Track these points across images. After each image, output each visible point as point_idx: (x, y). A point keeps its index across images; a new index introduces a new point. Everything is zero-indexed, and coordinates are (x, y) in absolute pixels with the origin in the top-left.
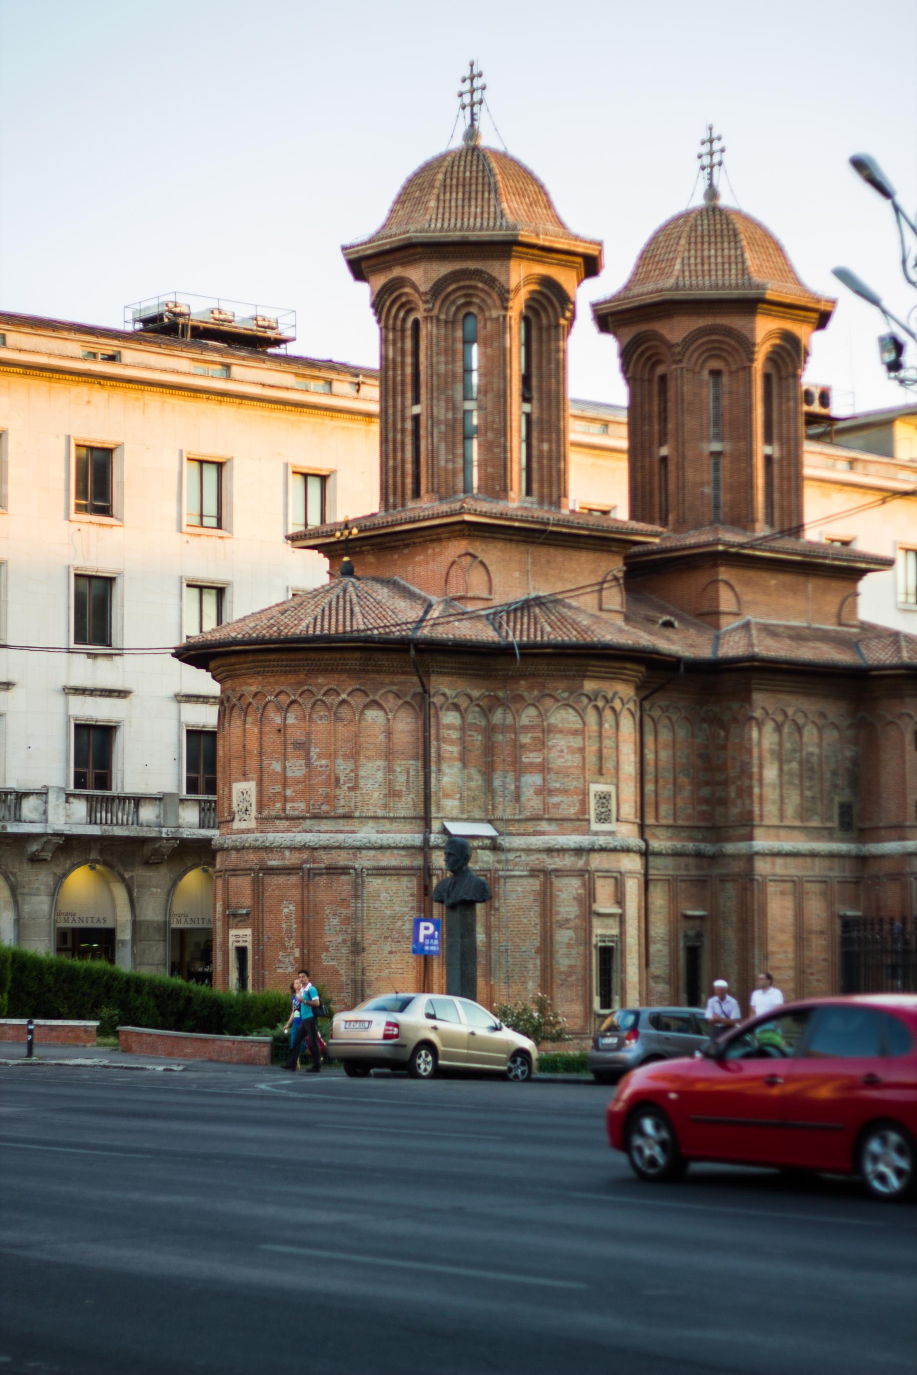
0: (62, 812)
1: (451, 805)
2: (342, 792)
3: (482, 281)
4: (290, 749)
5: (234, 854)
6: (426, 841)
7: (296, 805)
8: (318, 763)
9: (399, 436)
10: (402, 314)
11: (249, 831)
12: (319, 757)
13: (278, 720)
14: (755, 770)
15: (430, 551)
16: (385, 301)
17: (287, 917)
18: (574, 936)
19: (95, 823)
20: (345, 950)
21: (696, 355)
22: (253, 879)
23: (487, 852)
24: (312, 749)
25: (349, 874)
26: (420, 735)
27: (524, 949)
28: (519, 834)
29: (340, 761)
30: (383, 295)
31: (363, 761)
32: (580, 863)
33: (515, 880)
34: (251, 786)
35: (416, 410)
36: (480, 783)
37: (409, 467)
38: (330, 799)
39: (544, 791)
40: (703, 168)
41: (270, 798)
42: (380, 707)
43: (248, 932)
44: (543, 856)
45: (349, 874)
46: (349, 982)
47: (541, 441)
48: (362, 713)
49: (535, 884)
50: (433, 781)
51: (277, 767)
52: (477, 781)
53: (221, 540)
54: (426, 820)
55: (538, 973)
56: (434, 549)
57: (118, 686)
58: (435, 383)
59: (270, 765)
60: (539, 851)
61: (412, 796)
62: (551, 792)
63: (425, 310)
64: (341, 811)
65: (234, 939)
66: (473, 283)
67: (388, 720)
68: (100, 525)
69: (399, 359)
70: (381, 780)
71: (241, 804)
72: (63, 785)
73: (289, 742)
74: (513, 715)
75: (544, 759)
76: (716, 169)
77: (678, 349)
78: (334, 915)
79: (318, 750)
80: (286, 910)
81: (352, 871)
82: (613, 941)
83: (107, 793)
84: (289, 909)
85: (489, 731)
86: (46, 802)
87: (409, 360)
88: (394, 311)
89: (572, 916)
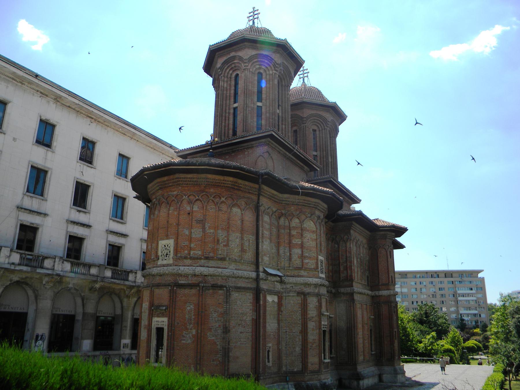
0: (60, 266)
1: (266, 259)
3: (267, 60)
5: (158, 278)
8: (209, 231)
9: (227, 115)
10: (231, 72)
11: (168, 265)
12: (210, 228)
13: (188, 209)
14: (352, 260)
15: (246, 153)
16: (225, 66)
17: (189, 312)
18: (314, 325)
19: (73, 273)
20: (220, 331)
21: (310, 123)
22: (170, 290)
23: (278, 284)
24: (206, 224)
25: (224, 290)
26: (255, 223)
27: (294, 332)
28: (291, 276)
29: (220, 231)
31: (231, 232)
32: (317, 291)
33: (290, 298)
34: (171, 242)
35: (235, 105)
36: (275, 251)
37: (231, 126)
39: (302, 257)
40: (300, 78)
41: (181, 248)
42: (239, 207)
43: (165, 319)
44: (302, 287)
45: (224, 290)
46: (221, 349)
47: (282, 124)
48: (231, 209)
49: (299, 300)
50: (260, 246)
52: (274, 251)
53: (126, 182)
54: (257, 264)
55: (301, 343)
56: (248, 152)
57: (87, 223)
58: (248, 92)
59: (183, 231)
60: (301, 284)
61: (251, 253)
62: (305, 257)
63: (245, 66)
64: (219, 256)
65: (156, 323)
66: (263, 60)
67: (242, 214)
68: (88, 166)
69: (228, 88)
70: (238, 243)
71: (163, 253)
72: (62, 256)
73: (194, 219)
74: (289, 221)
75: (302, 242)
76: (306, 79)
77: (305, 119)
78: (215, 311)
79: (209, 225)
80: (189, 308)
81: (225, 289)
82: (325, 328)
83: (79, 261)
84: (190, 307)
85: (279, 228)
86: (55, 262)
87: (233, 88)
88: (228, 70)
89: (314, 316)
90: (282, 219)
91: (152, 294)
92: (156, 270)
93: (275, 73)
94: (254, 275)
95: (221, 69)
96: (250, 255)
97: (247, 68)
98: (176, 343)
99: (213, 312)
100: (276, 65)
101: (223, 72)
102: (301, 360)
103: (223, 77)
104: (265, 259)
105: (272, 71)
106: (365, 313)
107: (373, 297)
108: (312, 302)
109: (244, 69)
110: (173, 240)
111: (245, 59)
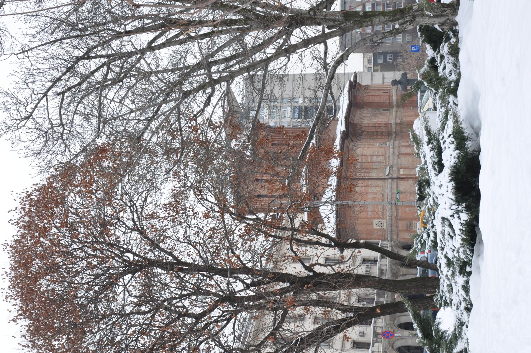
2: (377, 196)
5: (393, 228)
6: (390, 178)
11: (387, 223)
29: (369, 197)
34: (375, 221)
38: (379, 199)
39: (378, 156)
49: (402, 158)
51: (370, 213)
52: (375, 171)
60: (393, 157)
85: (362, 168)
90: (357, 166)
91: (402, 231)
94: (390, 181)
96: (380, 183)
104: (381, 175)
106: (409, 114)
107: (398, 107)
108: (404, 150)
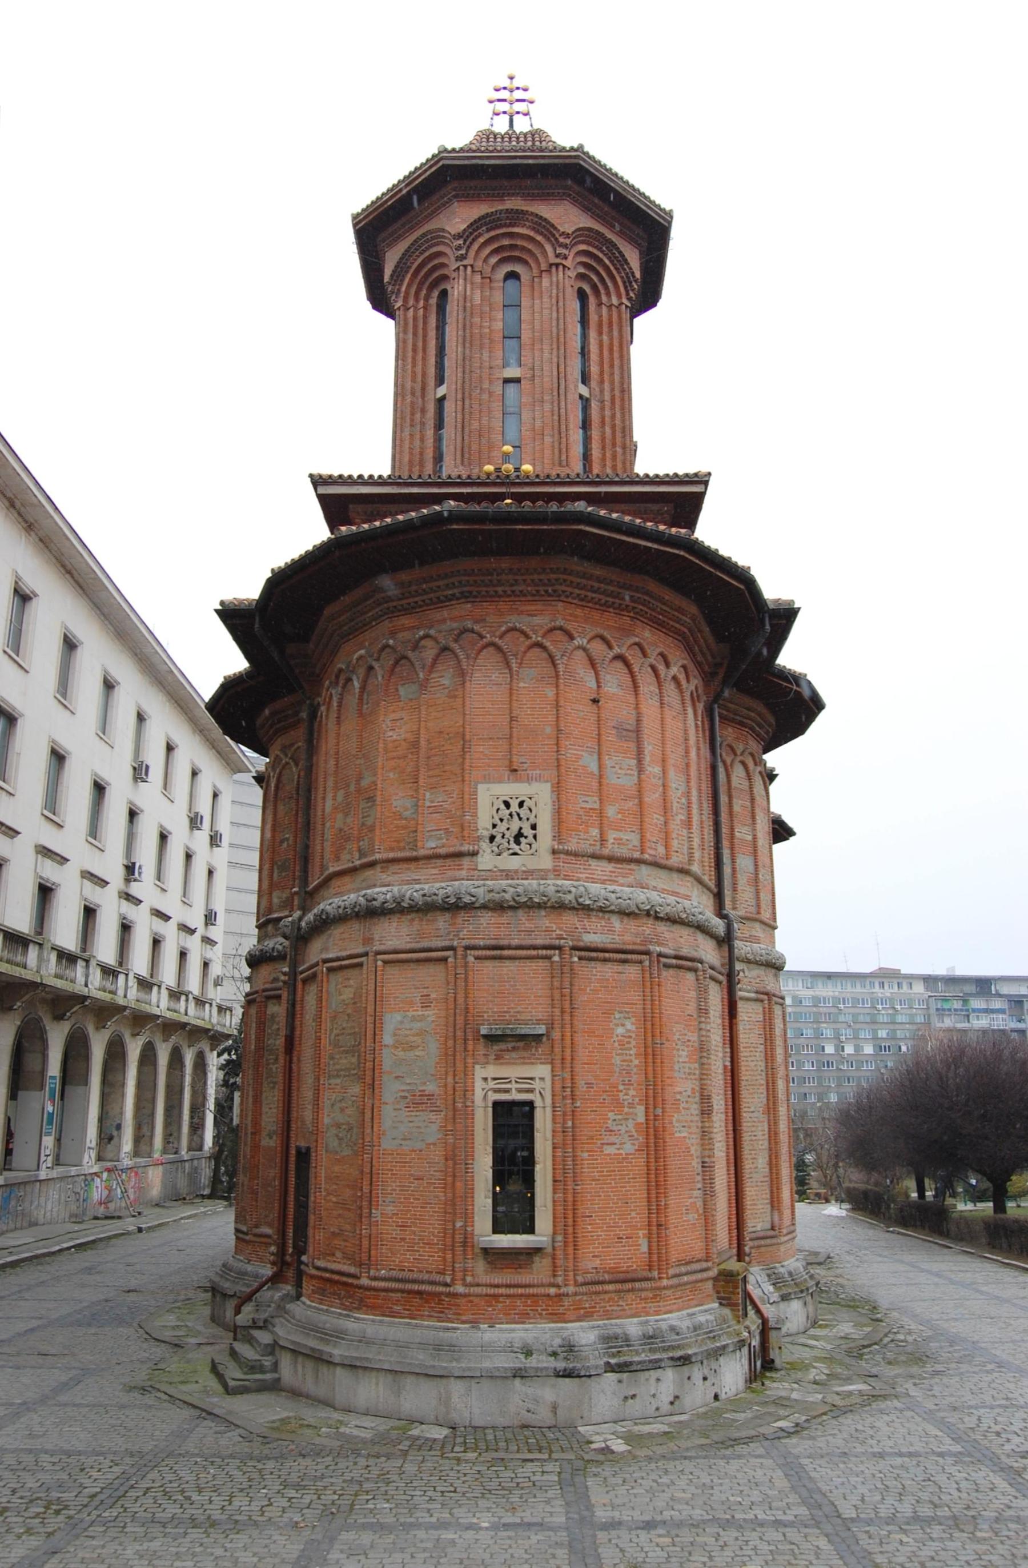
3: (609, 258)
4: (610, 737)
5: (486, 919)
7: (625, 836)
10: (493, 260)
11: (528, 874)
16: (480, 235)
20: (695, 1109)
27: (752, 1109)
30: (478, 228)
41: (579, 817)
43: (543, 1071)
59: (579, 758)
65: (492, 1084)
71: (502, 827)
80: (620, 1030)
84: (625, 1027)
88: (487, 250)
92: (481, 890)
93: (627, 306)
95: (465, 241)
97: (564, 262)
98: (586, 1155)
99: (679, 1043)
100: (634, 283)
101: (472, 253)
102: (768, 1196)
103: (469, 268)
105: (619, 296)
109: (551, 265)
110: (549, 785)
111: (563, 233)
